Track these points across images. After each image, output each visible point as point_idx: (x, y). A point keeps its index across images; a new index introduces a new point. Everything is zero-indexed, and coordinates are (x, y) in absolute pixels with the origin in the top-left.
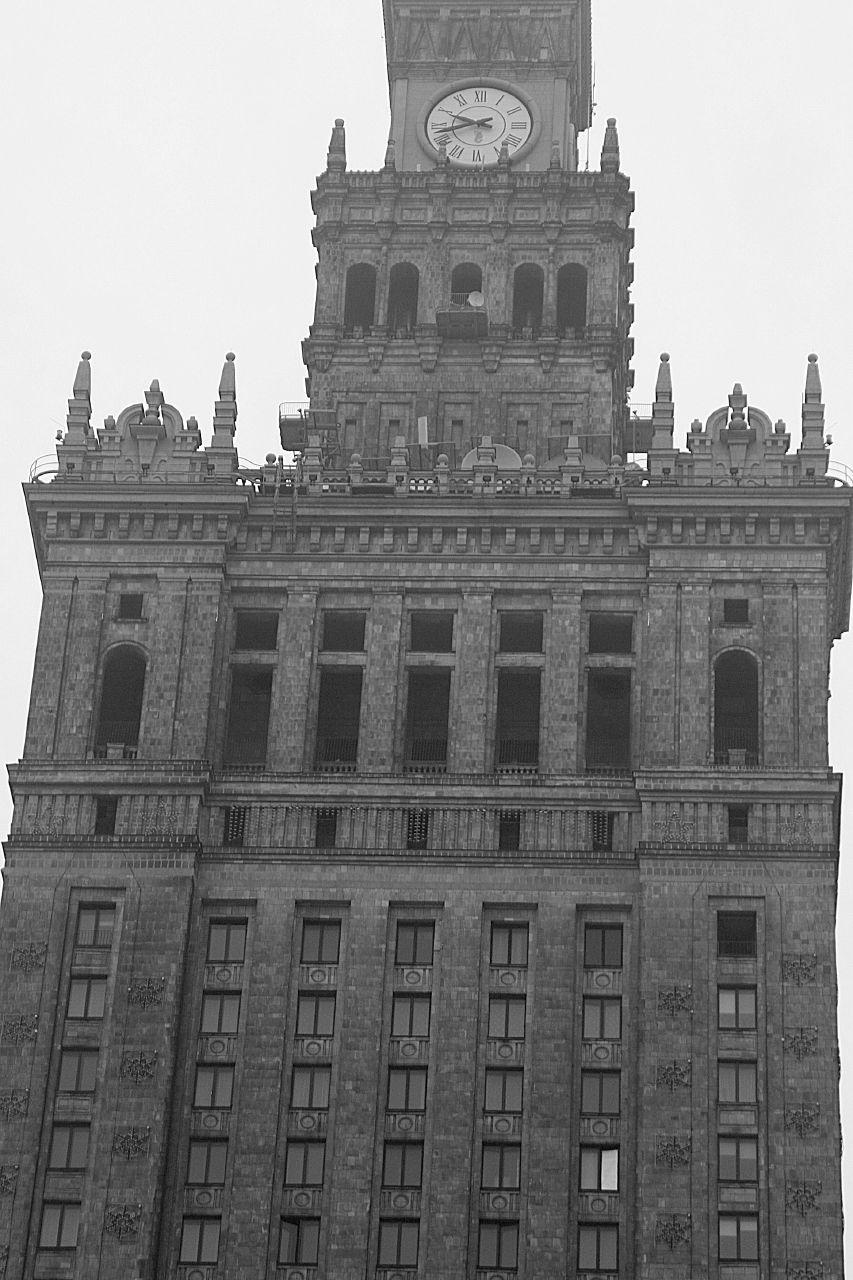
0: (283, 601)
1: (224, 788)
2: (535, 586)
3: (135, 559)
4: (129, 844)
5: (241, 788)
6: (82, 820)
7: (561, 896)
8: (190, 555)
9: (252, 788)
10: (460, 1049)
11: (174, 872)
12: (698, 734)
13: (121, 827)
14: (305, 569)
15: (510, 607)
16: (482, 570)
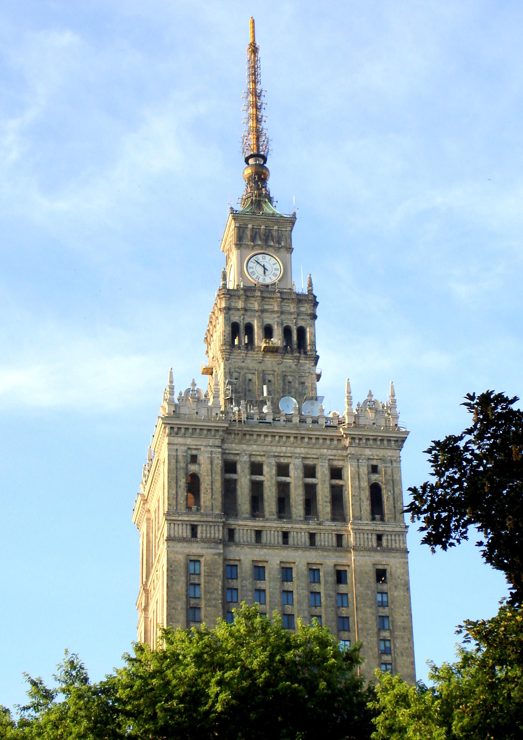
0: (238, 457)
1: (228, 522)
2: (314, 456)
3: (194, 443)
4: (203, 541)
5: (233, 522)
6: (187, 533)
7: (329, 561)
8: (211, 442)
9: (236, 523)
10: (304, 610)
11: (218, 551)
12: (366, 510)
13: (199, 535)
14: (245, 447)
15: (306, 463)
16: (298, 450)
